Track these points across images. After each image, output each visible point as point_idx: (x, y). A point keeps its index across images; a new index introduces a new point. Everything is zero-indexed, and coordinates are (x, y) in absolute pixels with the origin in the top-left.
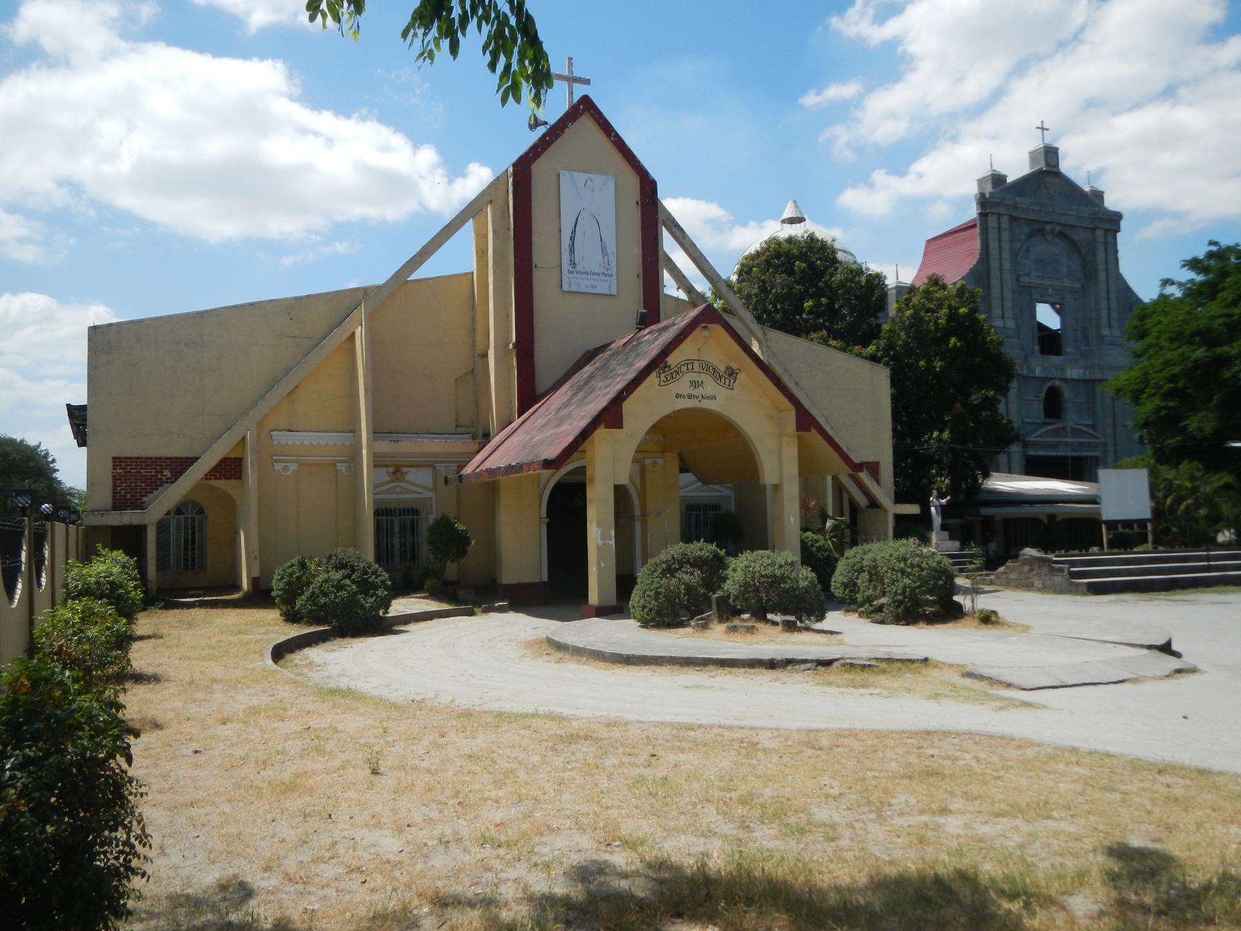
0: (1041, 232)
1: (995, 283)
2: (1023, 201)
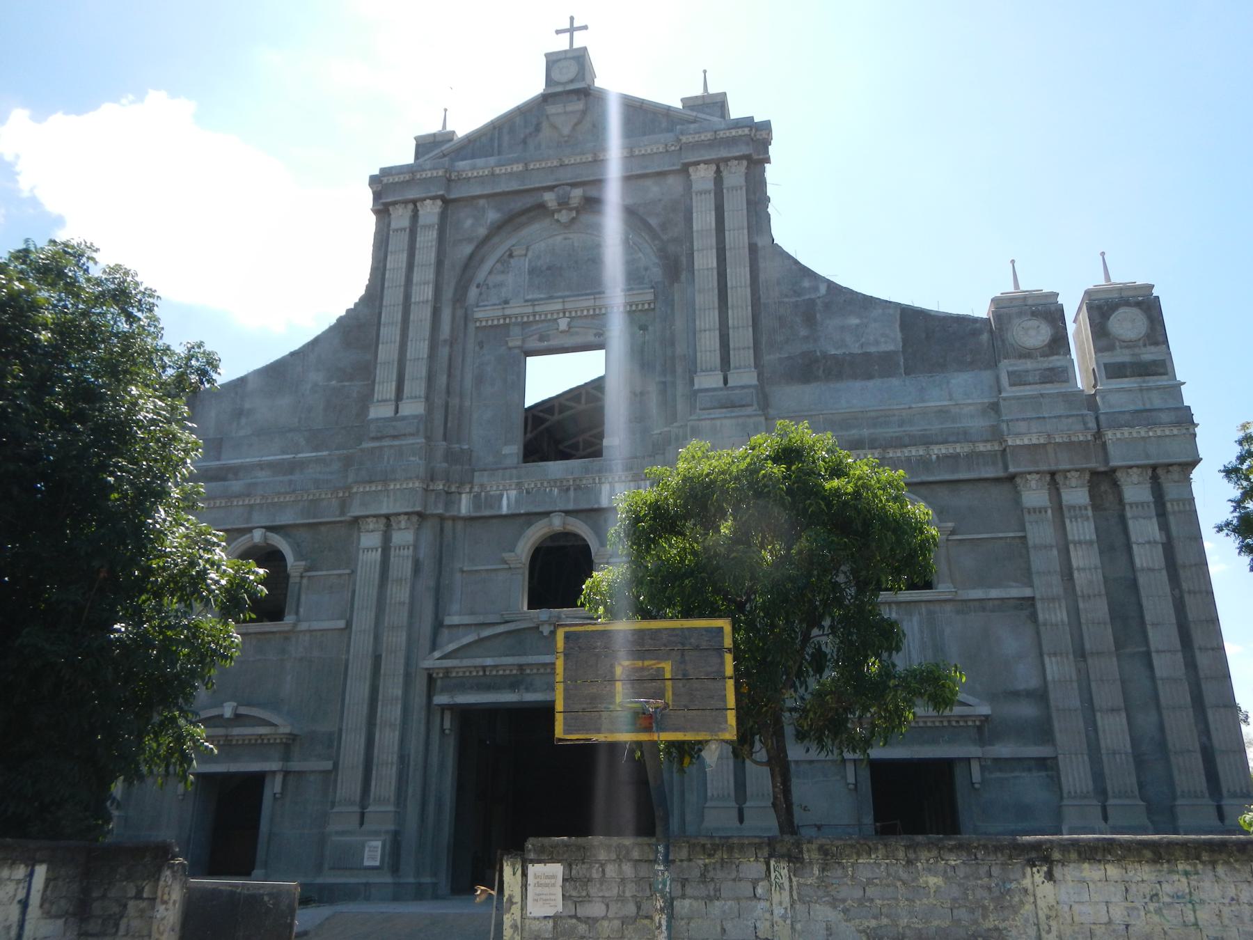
0: (540, 209)
1: (390, 332)
2: (482, 166)
